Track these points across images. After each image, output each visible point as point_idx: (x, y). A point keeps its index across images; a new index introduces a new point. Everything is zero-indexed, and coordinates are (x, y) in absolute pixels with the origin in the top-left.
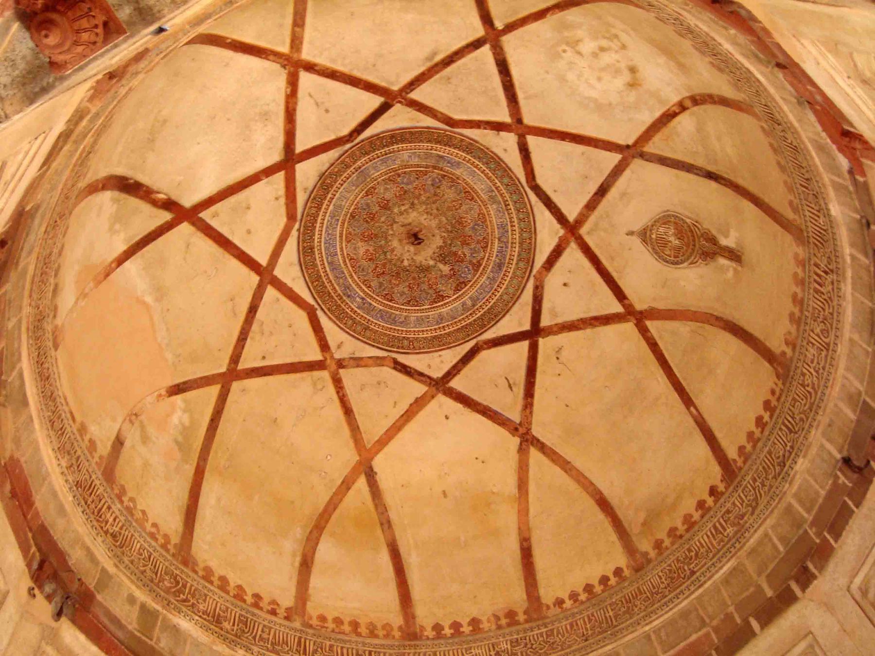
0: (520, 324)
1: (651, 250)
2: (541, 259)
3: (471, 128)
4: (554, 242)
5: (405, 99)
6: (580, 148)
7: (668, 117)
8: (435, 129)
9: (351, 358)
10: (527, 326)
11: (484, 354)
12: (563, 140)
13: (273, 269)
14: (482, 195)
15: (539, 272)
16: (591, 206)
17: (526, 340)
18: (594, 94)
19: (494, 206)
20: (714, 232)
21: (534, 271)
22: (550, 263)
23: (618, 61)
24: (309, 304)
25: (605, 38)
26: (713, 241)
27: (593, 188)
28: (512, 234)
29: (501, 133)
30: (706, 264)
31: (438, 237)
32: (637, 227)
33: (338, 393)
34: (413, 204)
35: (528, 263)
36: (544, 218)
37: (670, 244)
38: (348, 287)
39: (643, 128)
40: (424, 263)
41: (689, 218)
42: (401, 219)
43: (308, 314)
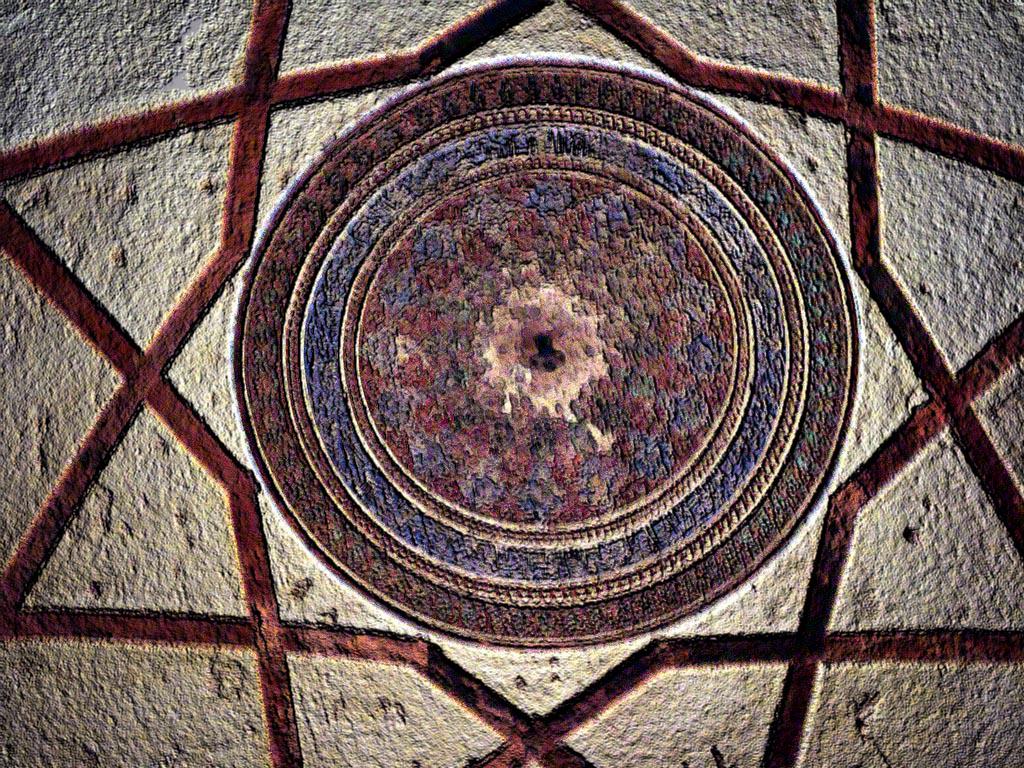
0: (771, 612)
4: (901, 415)
9: (323, 626)
10: (789, 624)
11: (664, 676)
13: (169, 362)
17: (782, 659)
21: (833, 488)
22: (873, 474)
24: (242, 468)
31: (601, 357)
33: (271, 713)
34: (551, 262)
35: (819, 460)
38: (348, 444)
40: (552, 410)
42: (513, 297)
43: (234, 496)
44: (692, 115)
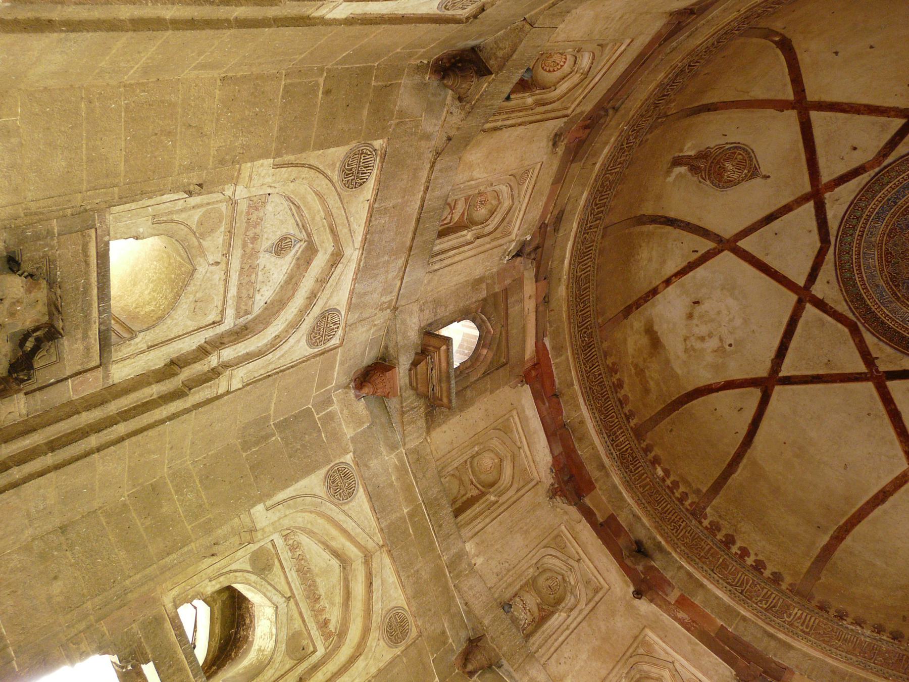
1: (754, 160)
2: (864, 178)
3: (841, 315)
5: (871, 370)
6: (767, 260)
7: (681, 273)
8: (868, 330)
12: (776, 272)
14: (876, 253)
15: (873, 167)
16: (787, 209)
18: (731, 302)
19: (873, 239)
20: (689, 174)
21: (877, 170)
23: (697, 325)
25: (694, 350)
26: (694, 169)
27: (776, 225)
28: (875, 209)
29: (821, 298)
30: (708, 148)
32: (758, 181)
36: (835, 212)
37: (734, 163)
39: (708, 263)
41: (707, 185)
44: (859, 313)
